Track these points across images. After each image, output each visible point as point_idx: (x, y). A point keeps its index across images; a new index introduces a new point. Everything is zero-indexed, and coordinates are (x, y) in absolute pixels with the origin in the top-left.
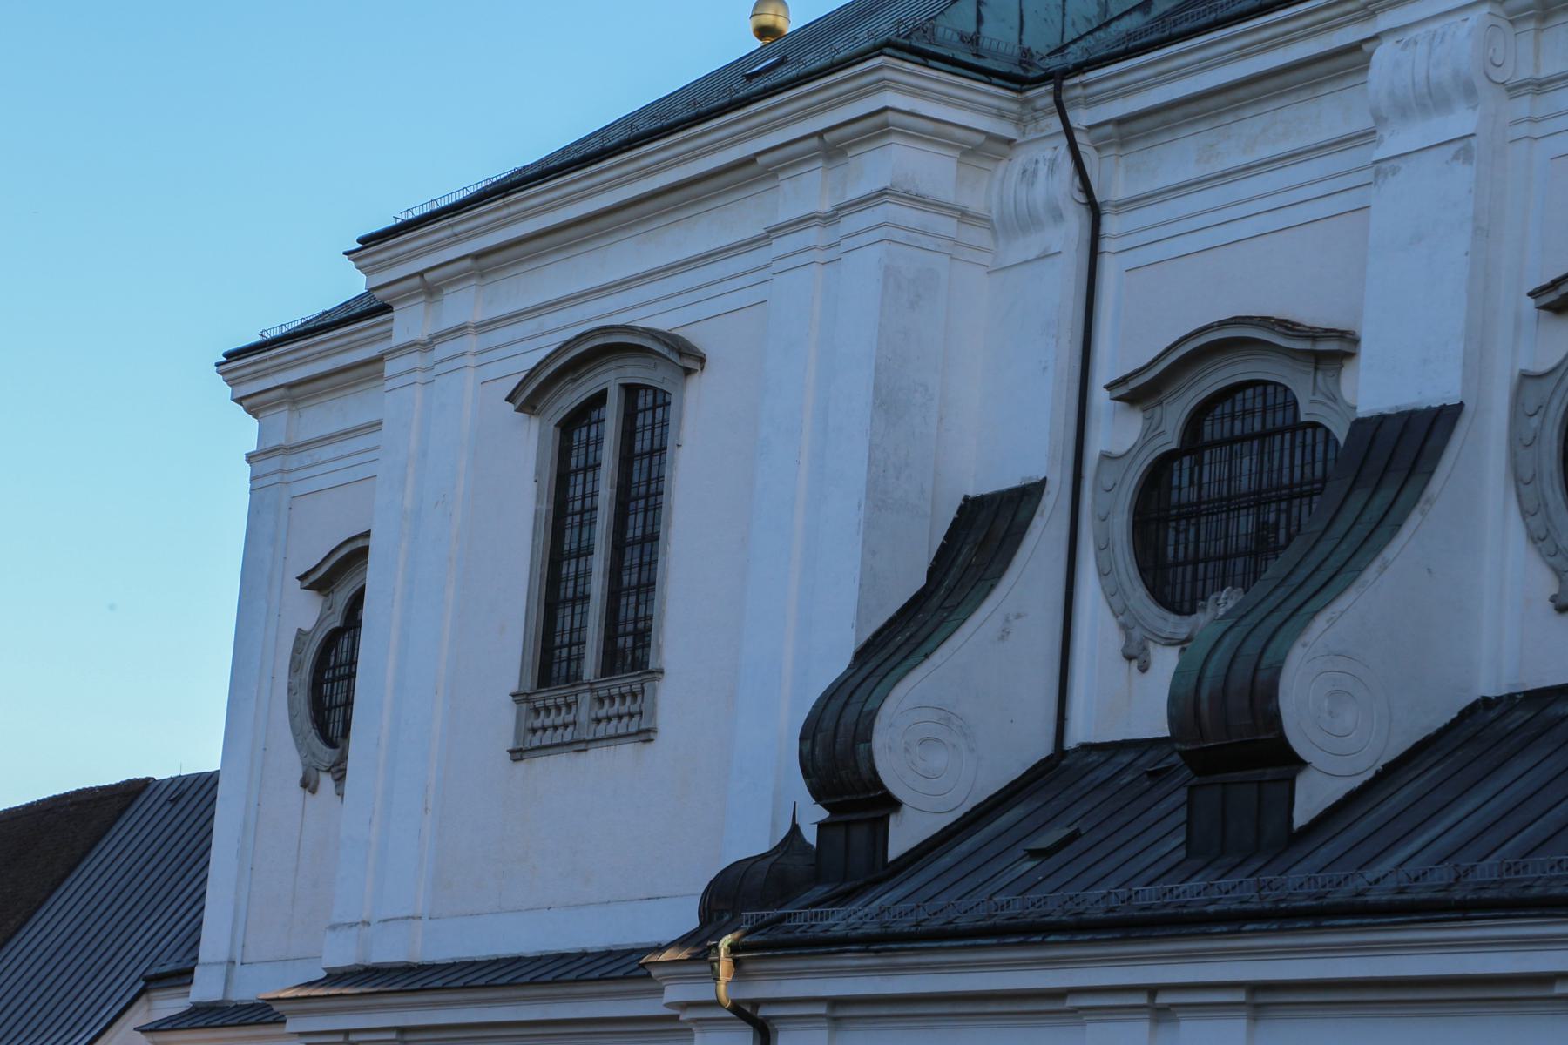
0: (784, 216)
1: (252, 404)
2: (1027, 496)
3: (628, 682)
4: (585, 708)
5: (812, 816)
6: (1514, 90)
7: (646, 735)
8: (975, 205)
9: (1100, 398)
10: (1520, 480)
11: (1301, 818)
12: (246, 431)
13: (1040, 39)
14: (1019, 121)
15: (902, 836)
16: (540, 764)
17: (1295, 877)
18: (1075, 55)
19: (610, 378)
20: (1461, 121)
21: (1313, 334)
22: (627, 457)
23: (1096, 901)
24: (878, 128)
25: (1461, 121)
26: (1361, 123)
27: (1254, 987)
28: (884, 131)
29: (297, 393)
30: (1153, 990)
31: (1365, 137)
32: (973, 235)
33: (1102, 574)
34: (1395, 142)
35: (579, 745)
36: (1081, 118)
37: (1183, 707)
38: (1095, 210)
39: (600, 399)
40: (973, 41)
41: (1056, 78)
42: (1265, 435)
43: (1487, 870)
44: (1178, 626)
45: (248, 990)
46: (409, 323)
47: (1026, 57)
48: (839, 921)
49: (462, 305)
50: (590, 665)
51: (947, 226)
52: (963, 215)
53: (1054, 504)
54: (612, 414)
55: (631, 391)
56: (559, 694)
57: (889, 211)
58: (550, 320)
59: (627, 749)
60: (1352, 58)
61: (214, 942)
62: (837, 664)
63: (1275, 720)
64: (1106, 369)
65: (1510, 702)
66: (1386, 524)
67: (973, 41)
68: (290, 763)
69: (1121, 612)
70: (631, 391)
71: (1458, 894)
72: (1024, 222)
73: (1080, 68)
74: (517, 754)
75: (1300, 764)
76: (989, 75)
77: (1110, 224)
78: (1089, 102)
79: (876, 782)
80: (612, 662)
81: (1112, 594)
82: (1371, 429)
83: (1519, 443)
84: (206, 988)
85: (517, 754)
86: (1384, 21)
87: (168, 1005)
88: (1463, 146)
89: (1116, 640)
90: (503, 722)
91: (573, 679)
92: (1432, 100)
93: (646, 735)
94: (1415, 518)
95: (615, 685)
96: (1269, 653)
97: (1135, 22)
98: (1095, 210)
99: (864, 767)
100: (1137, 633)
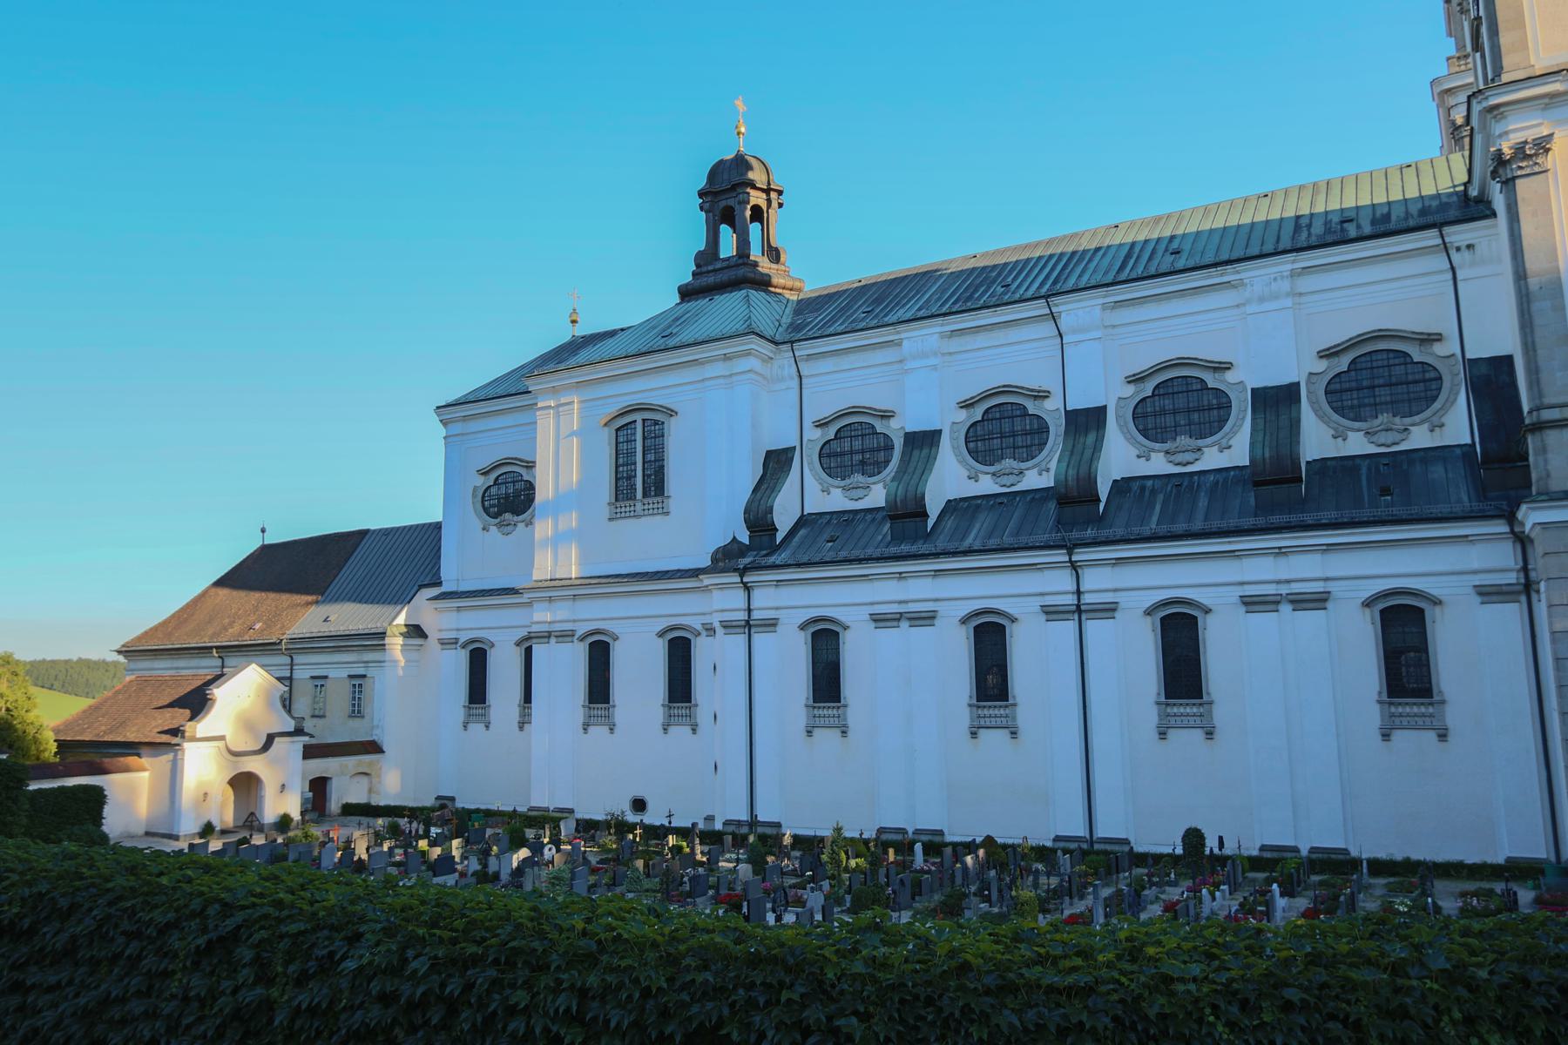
1: (444, 423)
2: (795, 447)
4: (639, 506)
5: (744, 537)
9: (807, 424)
12: (442, 431)
14: (775, 353)
16: (620, 522)
19: (638, 417)
20: (933, 361)
24: (748, 353)
25: (933, 361)
28: (749, 354)
30: (900, 573)
34: (909, 365)
36: (797, 354)
38: (800, 377)
42: (862, 435)
53: (798, 449)
55: (644, 420)
57: (751, 375)
59: (658, 518)
61: (445, 573)
70: (644, 420)
73: (799, 340)
77: (804, 381)
79: (773, 524)
81: (815, 475)
86: (903, 336)
87: (435, 591)
88: (934, 368)
90: (606, 512)
93: (667, 513)
95: (646, 501)
96: (919, 488)
98: (800, 377)
99: (769, 521)
100: (825, 485)
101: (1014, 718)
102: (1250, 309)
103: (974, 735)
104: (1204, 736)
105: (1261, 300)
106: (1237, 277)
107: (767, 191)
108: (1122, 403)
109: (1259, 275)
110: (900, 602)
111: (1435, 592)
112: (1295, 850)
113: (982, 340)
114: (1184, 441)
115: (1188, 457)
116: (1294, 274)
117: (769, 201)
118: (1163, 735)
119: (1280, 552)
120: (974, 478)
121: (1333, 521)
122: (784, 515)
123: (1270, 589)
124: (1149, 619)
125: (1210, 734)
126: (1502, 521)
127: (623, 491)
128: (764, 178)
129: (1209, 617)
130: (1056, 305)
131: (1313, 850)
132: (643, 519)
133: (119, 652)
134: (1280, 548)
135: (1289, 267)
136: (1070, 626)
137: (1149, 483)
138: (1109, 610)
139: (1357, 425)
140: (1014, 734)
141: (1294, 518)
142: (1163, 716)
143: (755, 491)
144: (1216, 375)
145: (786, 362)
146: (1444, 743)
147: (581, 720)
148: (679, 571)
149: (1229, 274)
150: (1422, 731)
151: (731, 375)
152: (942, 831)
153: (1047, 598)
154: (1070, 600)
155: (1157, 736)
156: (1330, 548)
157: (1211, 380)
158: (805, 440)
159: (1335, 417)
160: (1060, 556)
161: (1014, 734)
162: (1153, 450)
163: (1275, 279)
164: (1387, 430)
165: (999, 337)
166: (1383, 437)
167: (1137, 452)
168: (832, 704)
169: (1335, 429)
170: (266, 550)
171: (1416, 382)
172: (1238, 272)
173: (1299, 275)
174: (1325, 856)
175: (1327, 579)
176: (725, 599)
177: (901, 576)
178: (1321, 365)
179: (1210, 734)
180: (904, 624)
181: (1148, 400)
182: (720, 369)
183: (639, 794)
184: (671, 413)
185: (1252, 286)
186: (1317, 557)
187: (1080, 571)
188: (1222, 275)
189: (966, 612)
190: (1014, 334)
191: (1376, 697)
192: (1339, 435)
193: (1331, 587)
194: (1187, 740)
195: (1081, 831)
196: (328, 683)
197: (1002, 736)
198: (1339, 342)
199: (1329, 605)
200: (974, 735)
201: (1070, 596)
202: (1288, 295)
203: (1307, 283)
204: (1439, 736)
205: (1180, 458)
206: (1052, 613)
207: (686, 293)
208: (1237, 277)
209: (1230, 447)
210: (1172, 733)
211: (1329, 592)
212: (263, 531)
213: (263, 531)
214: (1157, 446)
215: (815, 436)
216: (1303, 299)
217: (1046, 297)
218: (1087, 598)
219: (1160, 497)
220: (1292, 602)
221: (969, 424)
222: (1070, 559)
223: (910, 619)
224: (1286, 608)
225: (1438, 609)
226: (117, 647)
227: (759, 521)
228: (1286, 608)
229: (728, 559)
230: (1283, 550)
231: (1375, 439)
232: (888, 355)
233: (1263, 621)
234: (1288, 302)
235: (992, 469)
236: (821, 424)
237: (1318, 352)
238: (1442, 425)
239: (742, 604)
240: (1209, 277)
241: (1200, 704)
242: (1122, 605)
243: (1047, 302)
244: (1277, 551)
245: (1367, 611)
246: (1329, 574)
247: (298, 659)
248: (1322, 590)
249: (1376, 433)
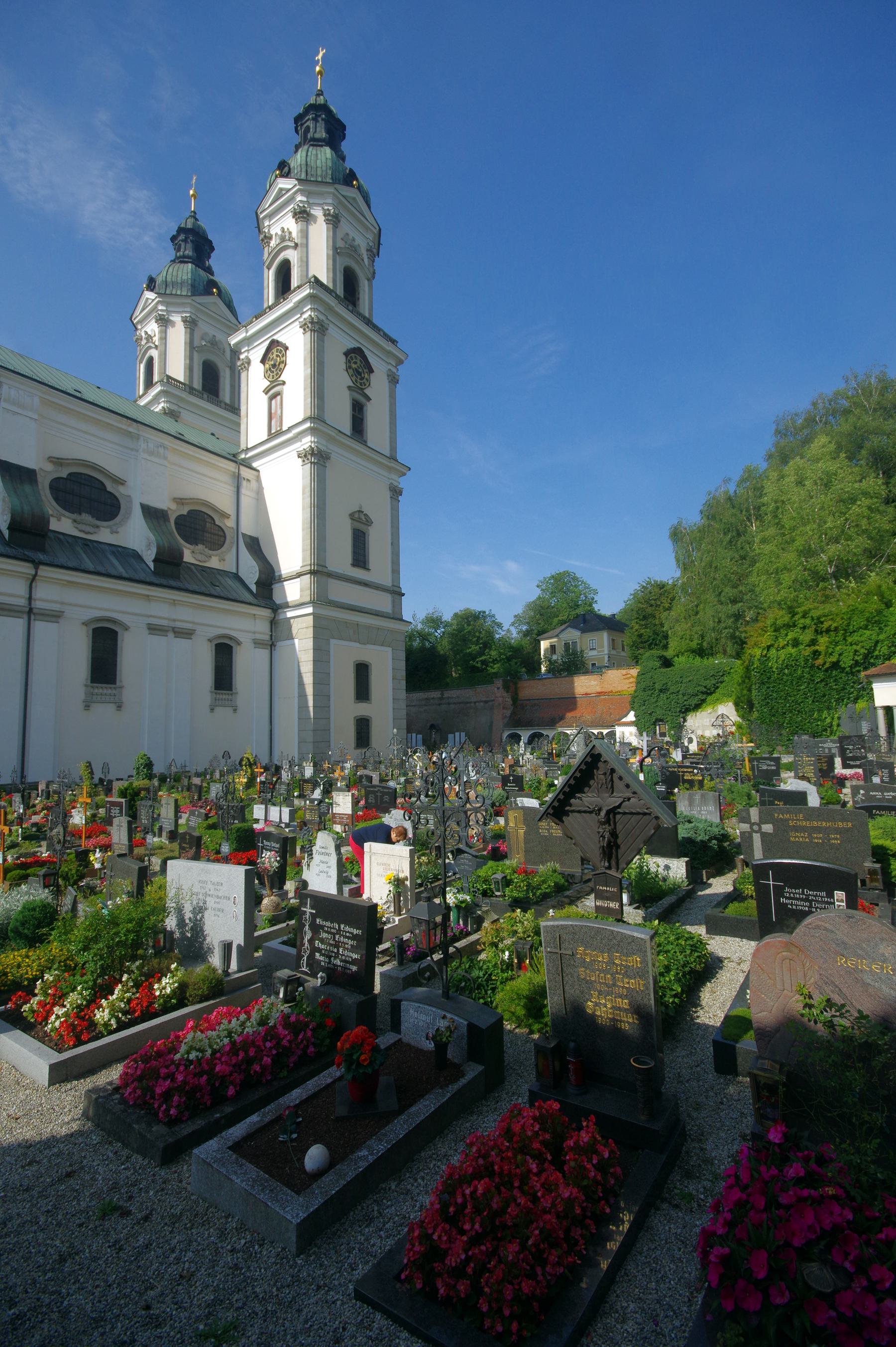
114: (86, 517)
115: (88, 529)
118: (87, 707)
119: (174, 603)
123: (164, 623)
126: (269, 611)
157: (110, 487)
162: (64, 516)
171: (214, 534)
205: (83, 527)
209: (117, 532)
214: (67, 514)
220: (175, 632)
228: (171, 635)
238: (224, 560)
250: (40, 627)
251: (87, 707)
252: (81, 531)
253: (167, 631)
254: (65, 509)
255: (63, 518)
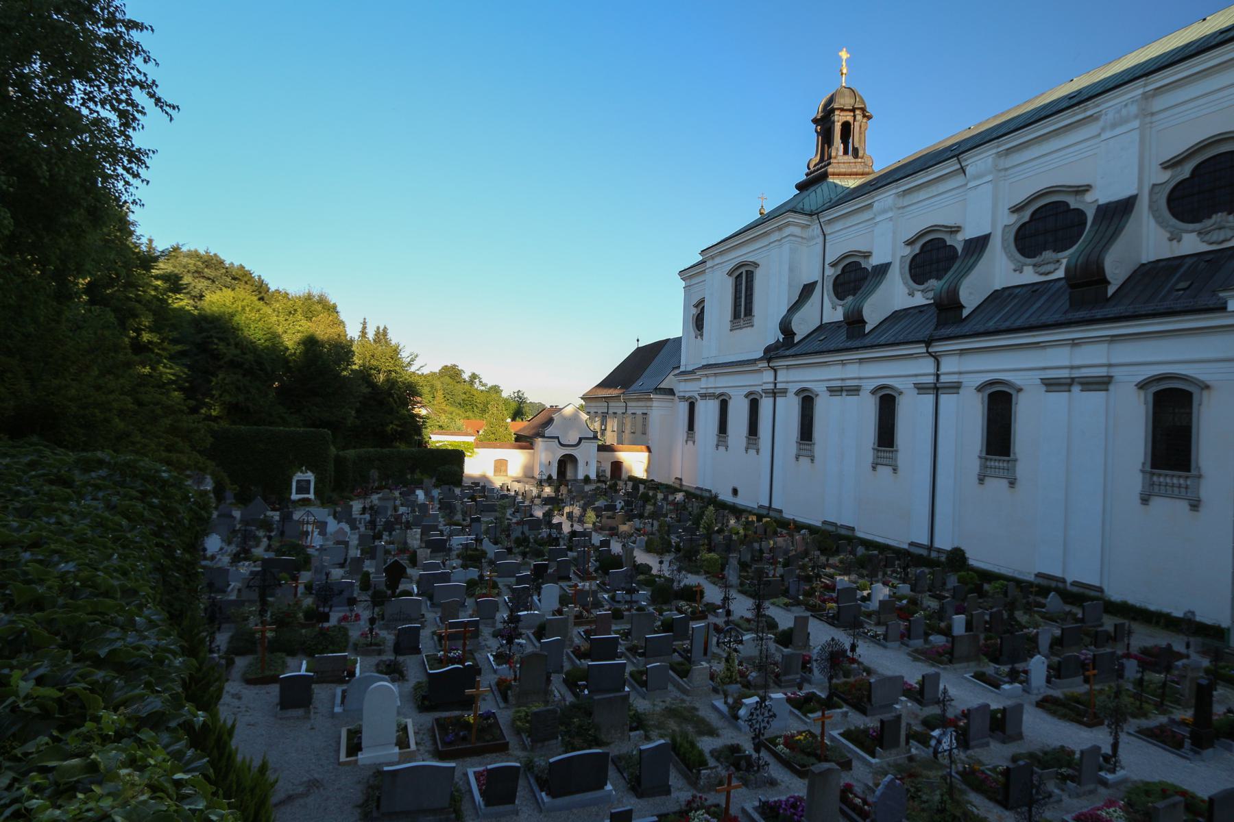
0: (772, 240)
2: (815, 283)
3: (749, 318)
5: (781, 337)
6: (899, 208)
7: (752, 326)
8: (804, 236)
9: (827, 266)
10: (902, 274)
11: (866, 332)
13: (814, 208)
15: (797, 339)
16: (735, 331)
17: (867, 341)
18: (819, 210)
19: (743, 270)
20: (890, 214)
21: (864, 253)
22: (747, 282)
23: (832, 347)
24: (788, 224)
26: (872, 216)
27: (860, 359)
29: (691, 277)
30: (842, 361)
31: (873, 218)
32: (805, 241)
33: (828, 295)
35: (741, 328)
36: (822, 220)
37: (846, 316)
39: (742, 273)
40: (803, 209)
41: (817, 214)
43: (901, 338)
44: (842, 303)
45: (690, 368)
46: (709, 264)
47: (812, 211)
48: (787, 353)
49: (718, 260)
50: (742, 316)
51: (800, 240)
52: (802, 238)
54: (744, 273)
55: (747, 271)
56: (738, 320)
58: (733, 261)
60: (870, 206)
62: (784, 312)
63: (862, 316)
64: (827, 262)
65: (901, 311)
66: (880, 283)
67: (803, 209)
68: (693, 334)
69: (831, 300)
70: (747, 271)
71: (897, 341)
72: (812, 238)
74: (731, 330)
75: (866, 323)
76: (806, 214)
77: (827, 237)
78: (824, 217)
79: (792, 331)
80: (745, 315)
82: (875, 268)
83: (901, 268)
84: (682, 369)
85: (731, 330)
86: (876, 199)
87: (677, 372)
88: (891, 219)
89: (830, 305)
90: (728, 325)
91: (740, 318)
92: (884, 211)
93: (752, 326)
94: (884, 282)
95: (746, 318)
97: (828, 204)
101: (896, 460)
102: (1104, 137)
103: (874, 468)
104: (1008, 485)
105: (1114, 126)
106: (1098, 109)
107: (853, 110)
108: (1007, 230)
109: (1111, 105)
110: (843, 379)
111: (1201, 377)
112: (1063, 581)
113: (922, 195)
115: (1050, 267)
116: (1146, 97)
117: (854, 116)
118: (981, 480)
119: (1074, 343)
120: (911, 294)
121: (1118, 315)
122: (803, 325)
123: (1064, 374)
124: (980, 395)
125: (1012, 483)
127: (736, 315)
128: (852, 101)
129: (1021, 395)
130: (966, 160)
131: (1075, 583)
132: (744, 329)
133: (582, 398)
134: (1073, 340)
135: (1140, 91)
136: (930, 398)
137: (1017, 291)
138: (955, 387)
139: (1191, 226)
140: (895, 470)
141: (1099, 314)
142: (984, 467)
143: (788, 311)
144: (1078, 197)
145: (816, 226)
146: (1195, 513)
147: (715, 443)
148: (748, 360)
149: (1091, 109)
150: (1177, 501)
151: (781, 239)
152: (854, 528)
153: (919, 378)
154: (931, 379)
155: (978, 481)
156: (1114, 339)
157: (1073, 203)
158: (825, 276)
159: (1174, 221)
160: (921, 349)
161: (895, 470)
163: (1126, 105)
164: (1220, 228)
165: (933, 190)
166: (1215, 236)
167: (1013, 267)
168: (997, 457)
169: (1171, 233)
170: (639, 349)
172: (1098, 106)
173: (1154, 96)
174: (1081, 590)
175: (1110, 365)
176: (766, 378)
177: (843, 363)
178: (1165, 176)
179: (1012, 483)
180: (844, 393)
181: (1027, 225)
182: (776, 236)
183: (736, 486)
184: (756, 265)
185: (1106, 115)
186: (1104, 347)
187: (940, 359)
188: (1085, 111)
189: (873, 387)
190: (942, 187)
191: (1140, 466)
192: (1175, 237)
193: (1114, 372)
194: (997, 485)
195: (924, 540)
196: (637, 416)
197: (888, 470)
198: (1180, 152)
199: (1111, 387)
200: (874, 468)
201: (932, 377)
202: (1136, 117)
203: (1159, 103)
204: (1191, 505)
206: (921, 388)
207: (802, 187)
208: (1098, 109)
210: (988, 480)
211: (1112, 377)
212: (638, 340)
213: (638, 340)
214: (1029, 261)
215: (830, 272)
216: (1155, 118)
217: (957, 156)
218: (943, 379)
219: (1016, 301)
220: (1081, 384)
221: (911, 257)
222: (927, 350)
223: (847, 391)
224: (1076, 389)
225: (1205, 393)
226: (581, 396)
227: (786, 329)
228: (1076, 389)
229: (772, 354)
230: (1076, 341)
231: (1207, 238)
232: (866, 215)
233: (1059, 398)
234: (1136, 124)
235: (922, 287)
236: (834, 265)
237: (1161, 164)
239: (772, 379)
240: (1075, 115)
241: (1008, 461)
242: (964, 384)
243: (958, 159)
244: (1071, 342)
245: (1142, 393)
246: (1114, 361)
247: (629, 404)
248: (1105, 374)
249: (1209, 232)
250: (944, 398)
251: (1145, 500)
252: (1041, 274)
253: (1071, 385)
254: (1183, 220)
255: (1025, 268)
